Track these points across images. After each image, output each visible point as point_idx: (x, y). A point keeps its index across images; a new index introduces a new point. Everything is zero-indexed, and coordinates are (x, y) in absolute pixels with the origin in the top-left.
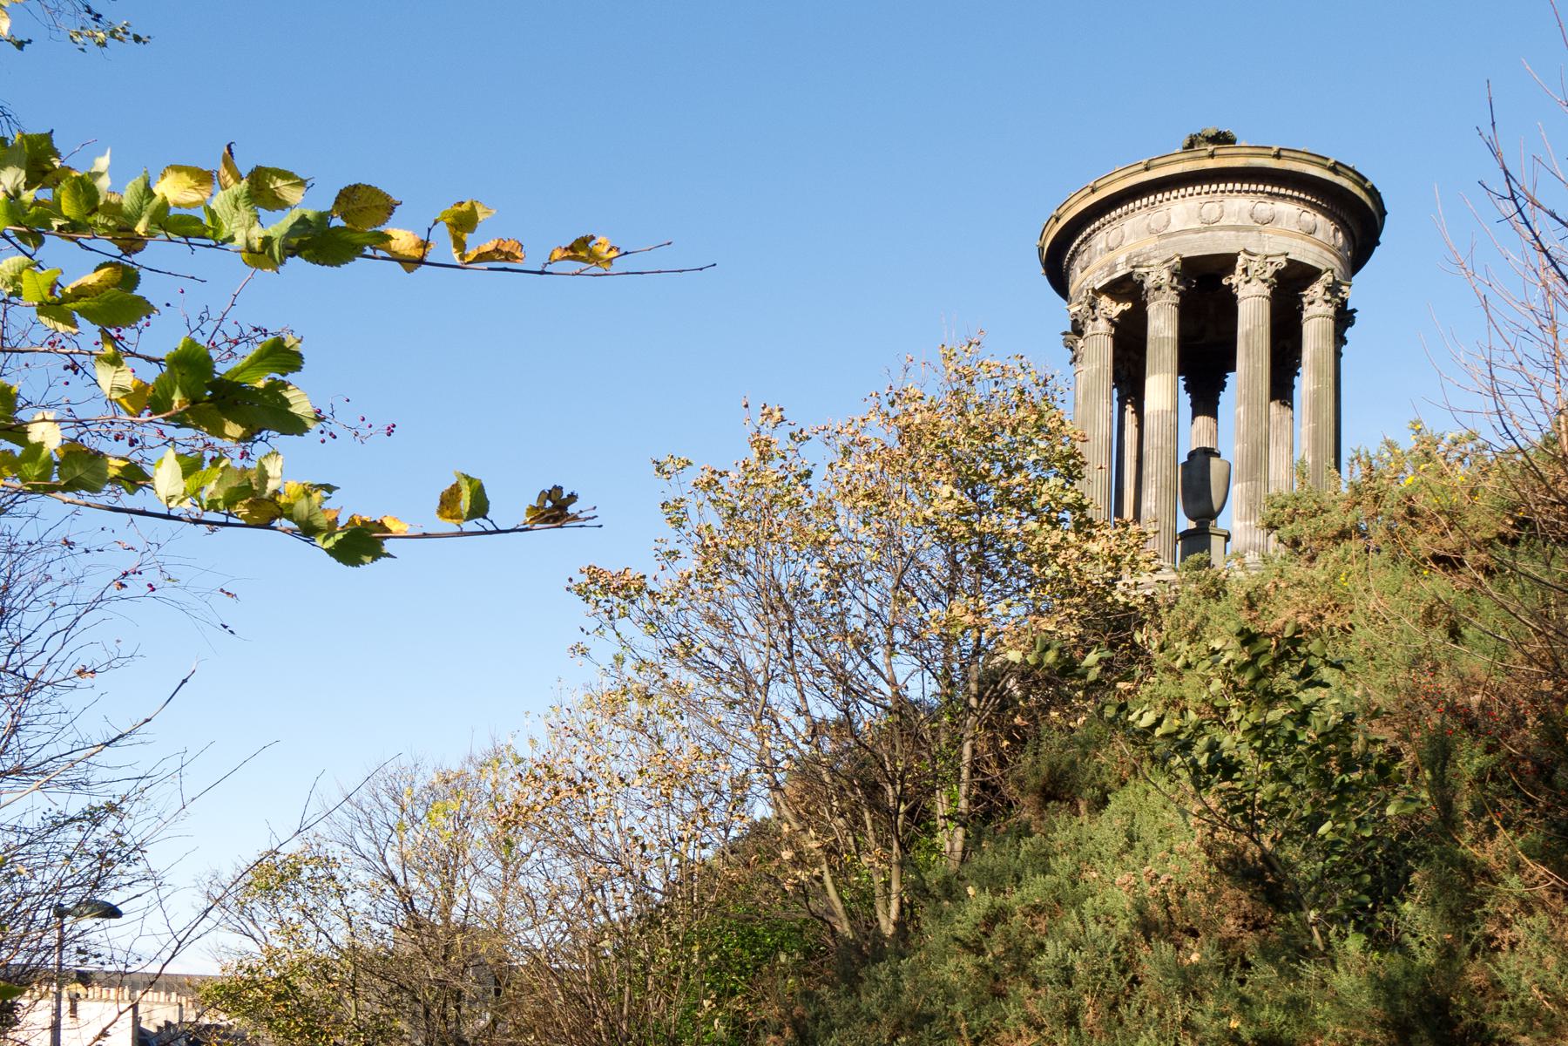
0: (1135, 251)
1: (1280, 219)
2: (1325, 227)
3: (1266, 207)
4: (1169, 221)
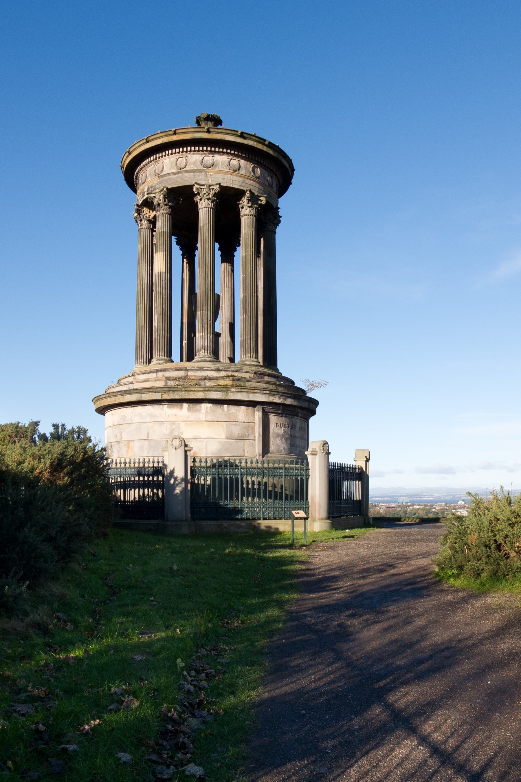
0: (150, 185)
1: (217, 165)
2: (246, 166)
3: (209, 159)
4: (163, 169)
